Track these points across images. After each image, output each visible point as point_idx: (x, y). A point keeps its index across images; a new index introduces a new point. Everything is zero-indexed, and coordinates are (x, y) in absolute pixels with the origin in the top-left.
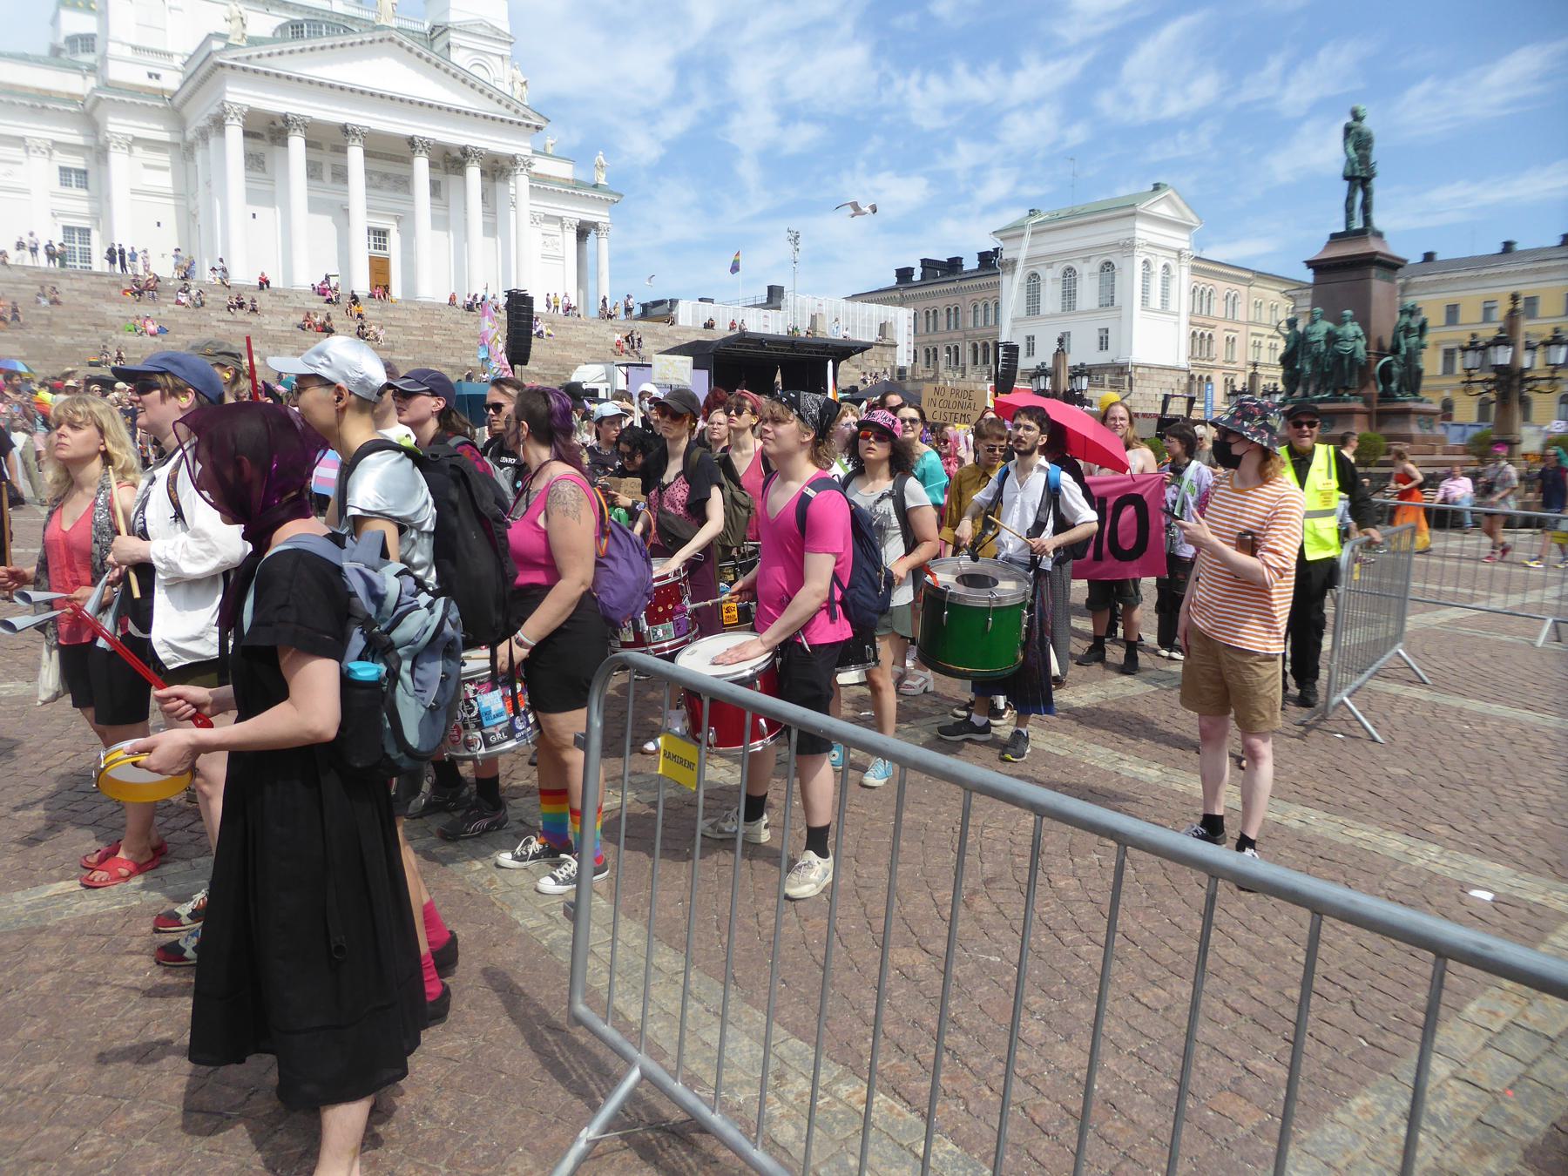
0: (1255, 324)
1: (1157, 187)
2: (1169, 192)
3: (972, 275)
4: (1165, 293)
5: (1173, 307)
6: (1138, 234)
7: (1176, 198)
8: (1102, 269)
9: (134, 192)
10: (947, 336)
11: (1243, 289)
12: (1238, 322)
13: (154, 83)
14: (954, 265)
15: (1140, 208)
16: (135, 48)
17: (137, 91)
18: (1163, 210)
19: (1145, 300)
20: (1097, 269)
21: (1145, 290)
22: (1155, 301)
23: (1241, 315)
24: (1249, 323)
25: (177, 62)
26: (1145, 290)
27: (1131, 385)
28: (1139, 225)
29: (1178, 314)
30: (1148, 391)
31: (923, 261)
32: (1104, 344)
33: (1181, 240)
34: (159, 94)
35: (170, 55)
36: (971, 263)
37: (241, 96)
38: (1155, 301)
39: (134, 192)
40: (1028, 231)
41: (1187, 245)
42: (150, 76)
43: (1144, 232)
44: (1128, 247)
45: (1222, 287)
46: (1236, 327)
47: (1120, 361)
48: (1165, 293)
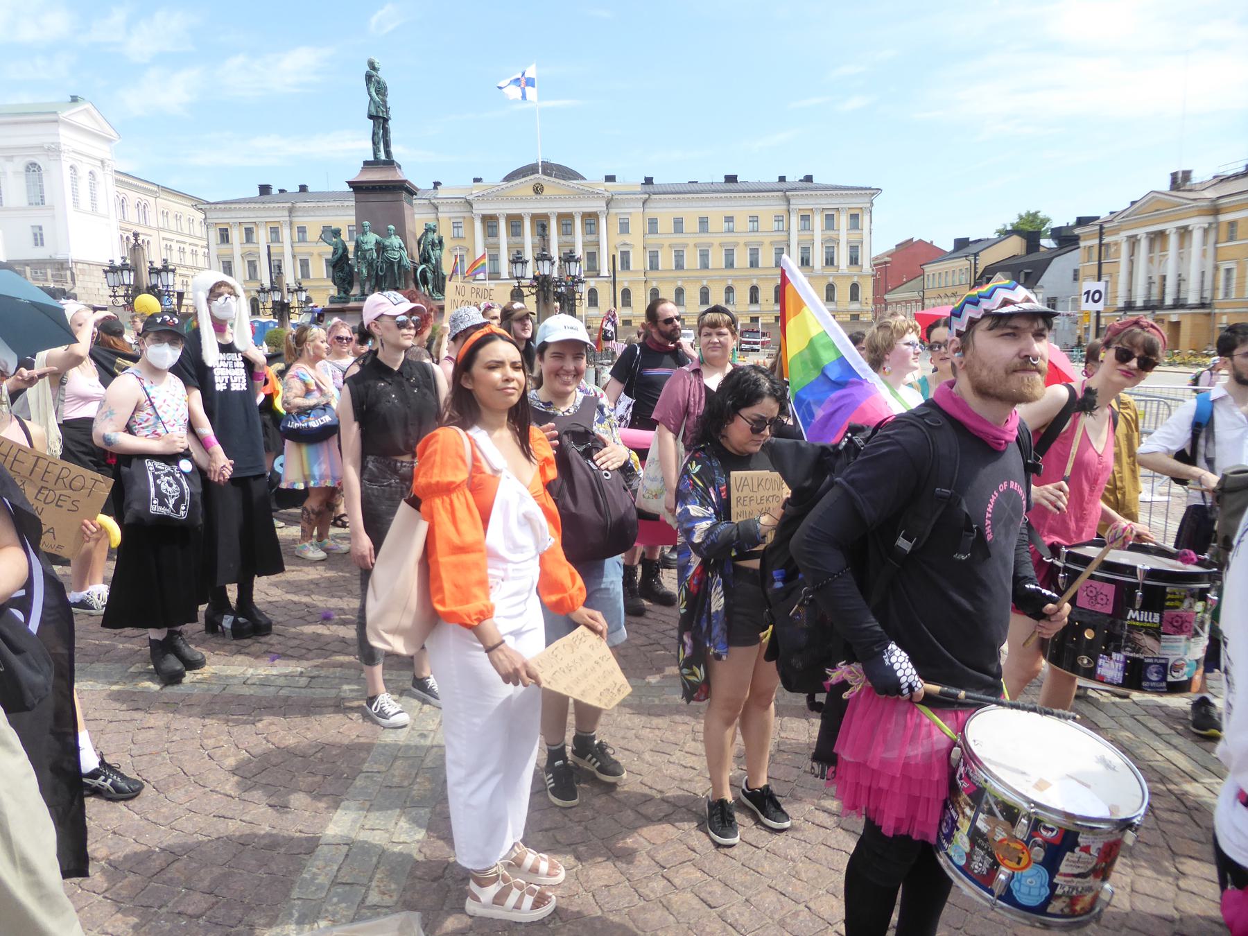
0: (164, 229)
1: (74, 99)
4: (93, 199)
6: (62, 140)
7: (95, 112)
8: (28, 169)
11: (152, 200)
12: (150, 228)
15: (63, 115)
19: (76, 203)
20: (22, 169)
21: (75, 192)
22: (85, 202)
26: (75, 192)
27: (73, 280)
28: (62, 131)
30: (90, 285)
32: (38, 239)
33: (102, 150)
38: (85, 202)
41: (109, 156)
43: (66, 137)
45: (133, 197)
46: (149, 232)
47: (60, 257)
48: (93, 199)
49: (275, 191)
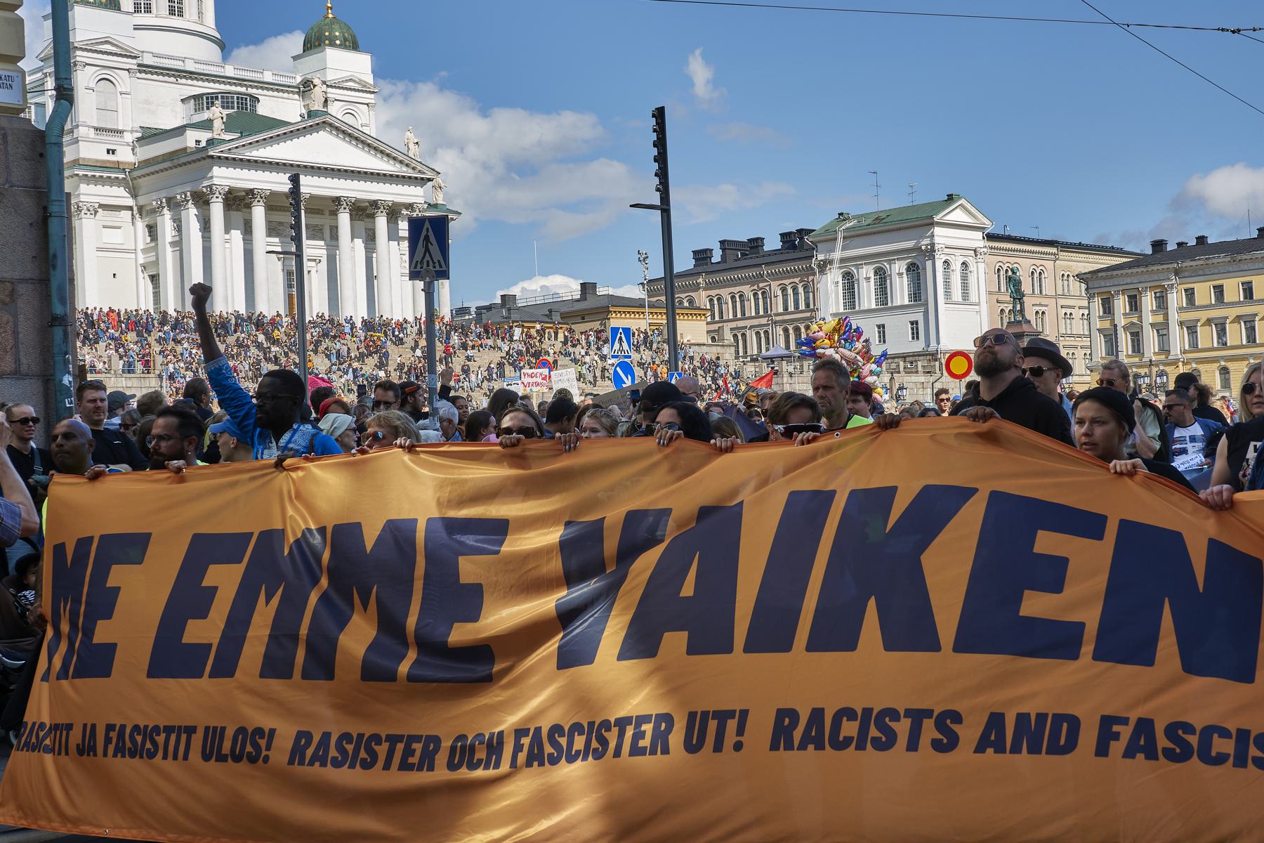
1: (950, 199)
2: (962, 201)
3: (774, 258)
4: (965, 286)
5: (973, 298)
7: (968, 206)
9: (99, 249)
10: (756, 322)
11: (1049, 264)
12: (1047, 296)
13: (111, 158)
14: (756, 243)
16: (96, 129)
17: (103, 166)
18: (957, 216)
23: (1048, 289)
24: (1056, 296)
25: (129, 137)
28: (938, 231)
29: (978, 304)
31: (722, 242)
34: (117, 167)
35: (121, 132)
36: (773, 243)
37: (224, 177)
38: (957, 294)
39: (99, 249)
40: (840, 236)
42: (108, 152)
44: (931, 252)
46: (1044, 301)
48: (965, 286)
49: (1171, 247)
